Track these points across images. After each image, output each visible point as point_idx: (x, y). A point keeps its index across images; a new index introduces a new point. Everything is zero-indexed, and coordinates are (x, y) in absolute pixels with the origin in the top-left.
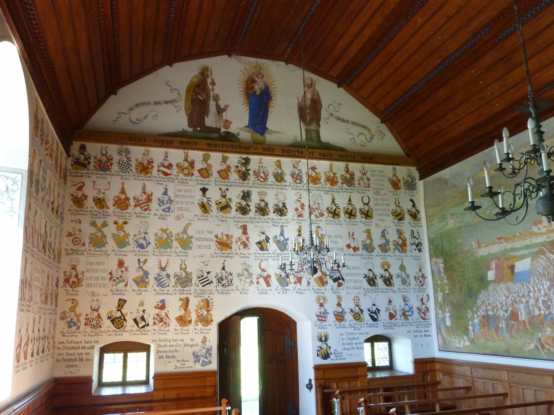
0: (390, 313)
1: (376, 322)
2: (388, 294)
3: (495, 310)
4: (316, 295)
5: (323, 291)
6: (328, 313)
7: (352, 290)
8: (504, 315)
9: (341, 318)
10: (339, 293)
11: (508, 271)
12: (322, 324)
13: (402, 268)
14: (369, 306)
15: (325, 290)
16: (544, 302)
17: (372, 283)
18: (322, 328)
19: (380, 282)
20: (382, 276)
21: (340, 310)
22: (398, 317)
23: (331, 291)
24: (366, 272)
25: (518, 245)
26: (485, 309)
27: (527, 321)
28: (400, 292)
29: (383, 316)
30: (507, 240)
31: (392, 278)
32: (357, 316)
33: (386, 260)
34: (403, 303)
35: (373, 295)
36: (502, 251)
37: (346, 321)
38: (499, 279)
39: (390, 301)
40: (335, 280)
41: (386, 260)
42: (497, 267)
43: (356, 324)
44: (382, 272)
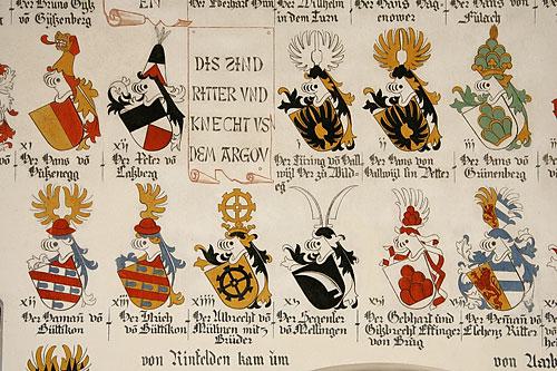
0: (407, 270)
1: (328, 312)
2: (403, 182)
4: (39, 184)
5: (73, 166)
7: (219, 164)
9: (155, 288)
10: (154, 175)
12: (55, 313)
13: (492, 60)
14: (303, 236)
15: (86, 161)
17: (321, 132)
18: (58, 330)
19: (365, 129)
20: (379, 99)
21: (152, 250)
22: (449, 288)
23: (112, 168)
24: (297, 81)
28: (467, 173)
29: (373, 283)
31: (429, 108)
32: (237, 279)
33: (404, 25)
34: (479, 230)
35: (325, 189)
37: (179, 300)
39: (412, 219)
40: (133, 120)
41: (404, 25)
43: (226, 317)
44: (381, 80)
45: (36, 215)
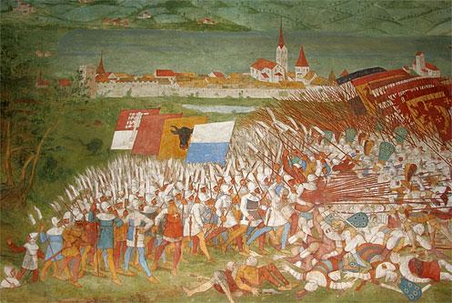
3: (121, 213)
8: (143, 224)
11: (169, 138)
16: (250, 204)
25: (209, 93)
26: (88, 207)
27: (202, 239)
30: (180, 78)
36: (165, 97)
38: (144, 150)
42: (144, 126)
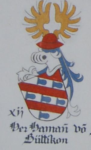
6: (77, 78)
45: (28, 30)
